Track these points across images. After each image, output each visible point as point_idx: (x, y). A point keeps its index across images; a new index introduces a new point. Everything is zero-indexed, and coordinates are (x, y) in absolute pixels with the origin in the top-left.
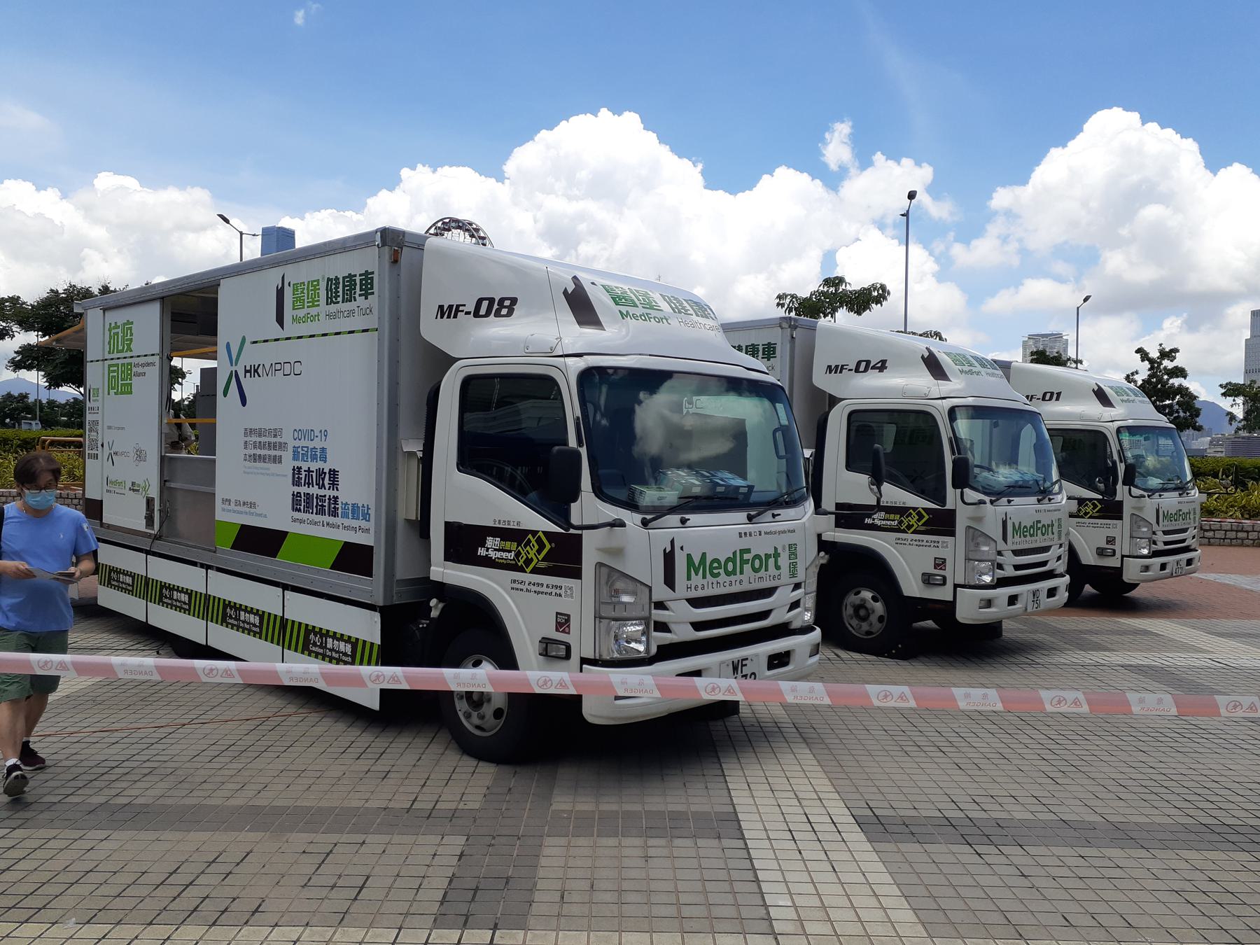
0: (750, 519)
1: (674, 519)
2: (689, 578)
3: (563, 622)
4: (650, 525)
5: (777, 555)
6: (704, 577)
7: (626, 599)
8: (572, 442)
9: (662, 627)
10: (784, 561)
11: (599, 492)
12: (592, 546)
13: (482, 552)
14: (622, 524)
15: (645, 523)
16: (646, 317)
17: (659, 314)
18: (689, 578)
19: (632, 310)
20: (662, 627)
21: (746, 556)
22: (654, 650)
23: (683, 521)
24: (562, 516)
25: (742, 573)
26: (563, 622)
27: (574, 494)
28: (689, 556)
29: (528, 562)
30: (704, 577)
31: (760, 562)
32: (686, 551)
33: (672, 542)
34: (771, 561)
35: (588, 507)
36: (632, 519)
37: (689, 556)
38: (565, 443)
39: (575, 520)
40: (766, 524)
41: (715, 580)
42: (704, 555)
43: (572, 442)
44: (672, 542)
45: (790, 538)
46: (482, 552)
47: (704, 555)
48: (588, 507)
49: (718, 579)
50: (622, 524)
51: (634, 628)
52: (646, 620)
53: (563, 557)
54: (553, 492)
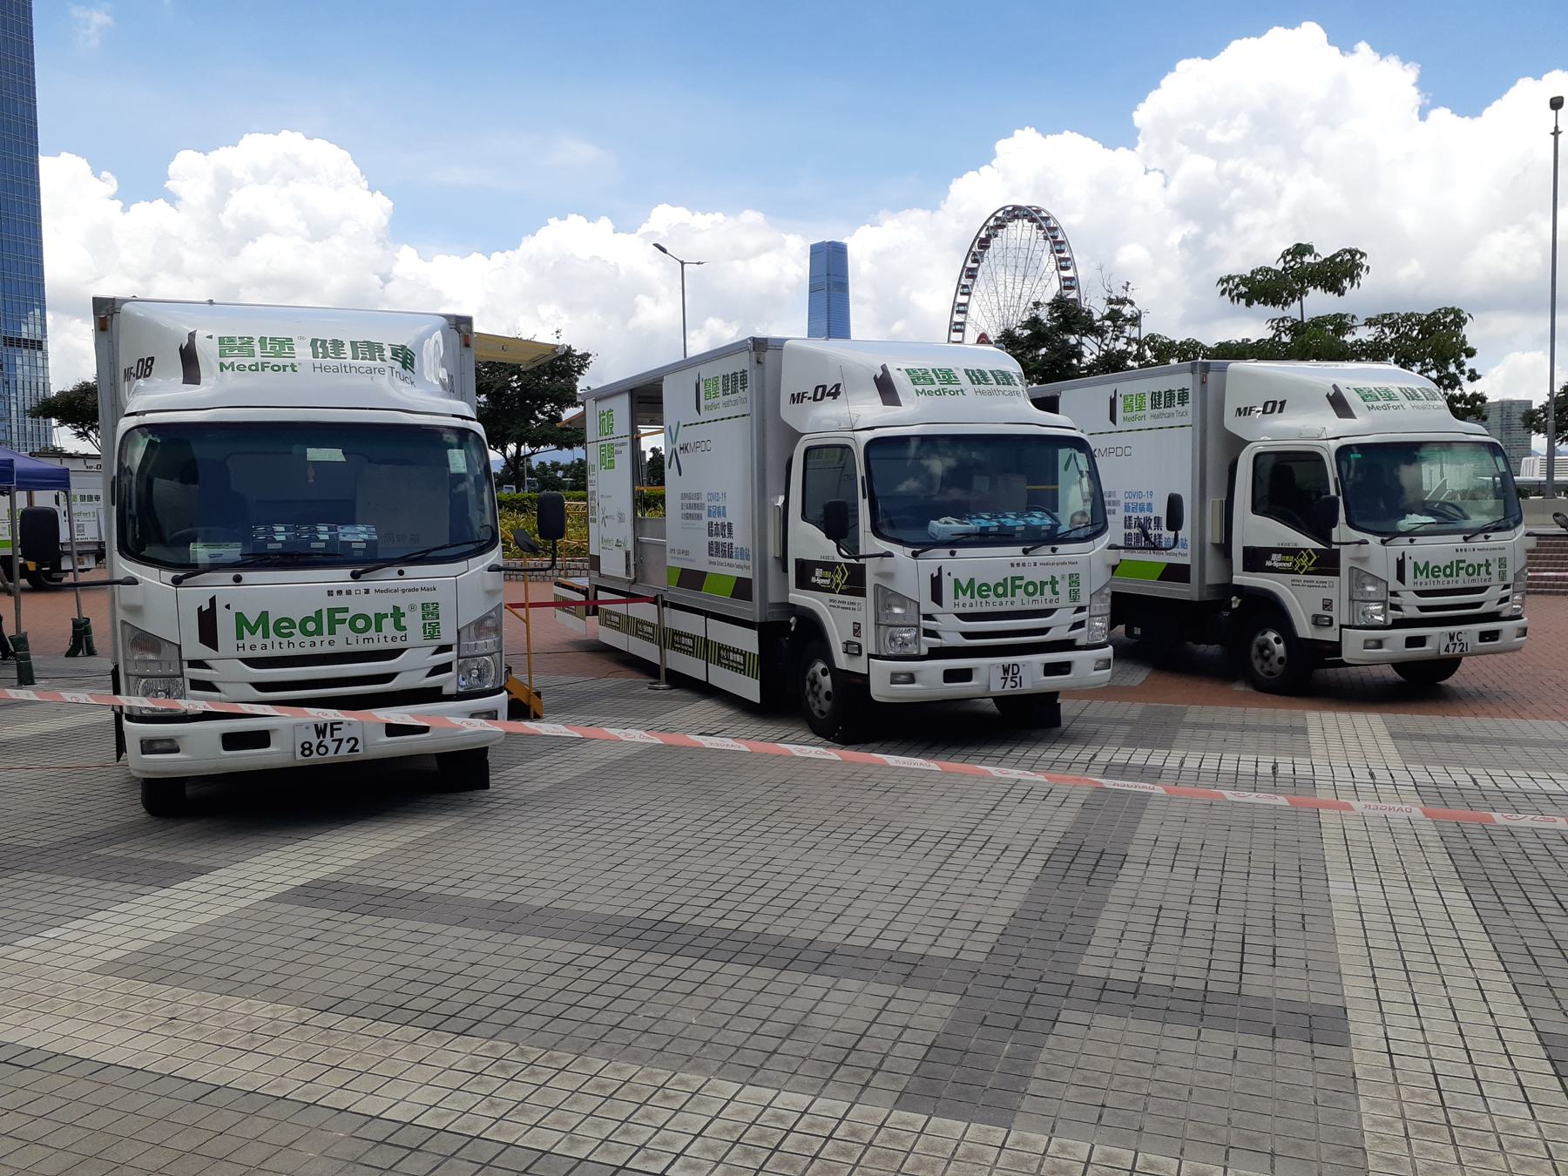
3: (1327, 605)
5: (1488, 564)
7: (1369, 589)
8: (1333, 493)
9: (1396, 607)
10: (1494, 569)
12: (1346, 556)
13: (1268, 563)
14: (1366, 542)
15: (1383, 542)
16: (1387, 408)
17: (1396, 403)
19: (1376, 404)
20: (1396, 607)
22: (1390, 622)
24: (1324, 537)
26: (1327, 605)
27: (1334, 522)
29: (1301, 568)
34: (1483, 569)
35: (1342, 532)
36: (1374, 540)
38: (1328, 492)
39: (1335, 538)
40: (1479, 542)
43: (1333, 493)
46: (1268, 563)
50: (1366, 542)
51: (1374, 607)
52: (1384, 602)
53: (1327, 563)
54: (1320, 526)
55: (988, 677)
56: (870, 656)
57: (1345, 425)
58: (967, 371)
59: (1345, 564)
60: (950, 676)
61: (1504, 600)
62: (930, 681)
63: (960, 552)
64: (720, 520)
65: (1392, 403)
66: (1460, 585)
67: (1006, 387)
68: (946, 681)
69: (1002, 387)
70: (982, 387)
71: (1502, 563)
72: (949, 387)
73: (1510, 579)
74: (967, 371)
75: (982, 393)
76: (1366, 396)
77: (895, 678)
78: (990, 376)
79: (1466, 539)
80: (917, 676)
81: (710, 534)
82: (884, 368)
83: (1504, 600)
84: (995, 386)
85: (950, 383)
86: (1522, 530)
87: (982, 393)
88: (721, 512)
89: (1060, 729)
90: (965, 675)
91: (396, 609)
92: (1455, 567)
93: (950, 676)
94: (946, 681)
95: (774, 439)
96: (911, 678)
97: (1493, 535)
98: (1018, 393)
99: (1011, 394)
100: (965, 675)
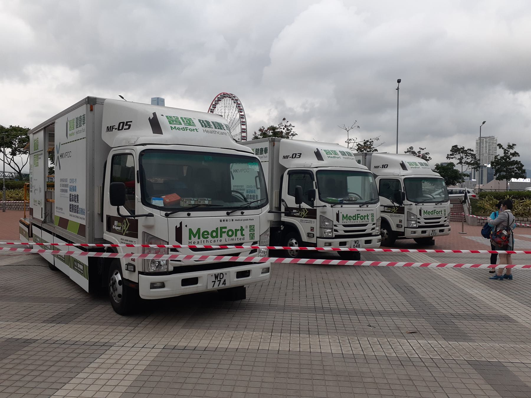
0: (228, 214)
1: (185, 214)
2: (190, 239)
4: (230, 215)
5: (368, 216)
6: (199, 238)
10: (370, 217)
11: (320, 199)
18: (190, 239)
21: (223, 230)
23: (189, 215)
25: (221, 237)
28: (190, 230)
30: (199, 238)
31: (438, 213)
32: (189, 227)
33: (181, 223)
37: (190, 230)
40: (364, 207)
41: (205, 240)
42: (199, 229)
44: (181, 223)
45: (372, 212)
47: (199, 229)
48: (140, 208)
49: (207, 239)
55: (206, 281)
56: (140, 273)
57: (320, 163)
58: (200, 121)
59: (406, 210)
60: (185, 282)
61: (373, 229)
62: (173, 286)
63: (193, 213)
64: (73, 193)
65: (336, 156)
66: (358, 223)
67: (220, 130)
68: (183, 285)
69: (217, 130)
70: (207, 129)
71: (372, 215)
72: (190, 127)
73: (447, 215)
74: (200, 121)
75: (207, 132)
76: (327, 152)
77: (153, 286)
78: (211, 124)
79: (360, 206)
80: (166, 284)
81: (70, 201)
82: (154, 114)
83: (373, 229)
84: (214, 129)
85: (190, 125)
86: (379, 204)
87: (207, 132)
88: (74, 189)
89: (244, 301)
90: (194, 281)
91: (242, 227)
92: (356, 217)
93: (185, 282)
94: (183, 285)
95: (98, 148)
96: (163, 285)
97: (370, 206)
98: (225, 134)
99: (222, 134)
100: (194, 281)
